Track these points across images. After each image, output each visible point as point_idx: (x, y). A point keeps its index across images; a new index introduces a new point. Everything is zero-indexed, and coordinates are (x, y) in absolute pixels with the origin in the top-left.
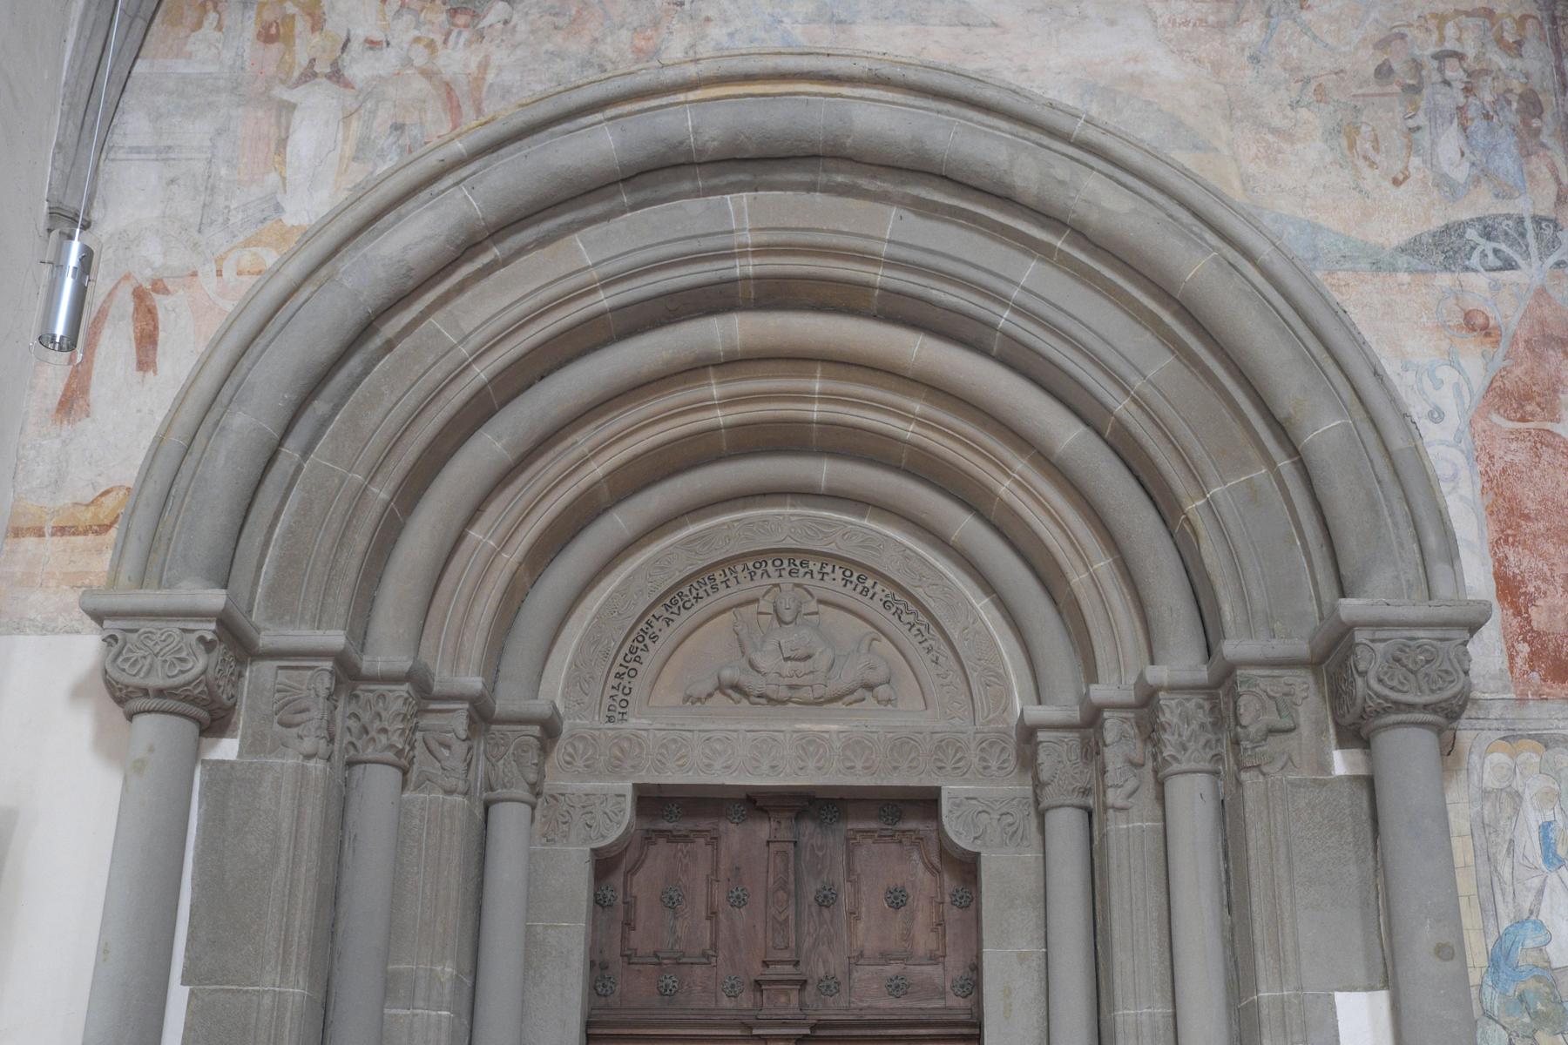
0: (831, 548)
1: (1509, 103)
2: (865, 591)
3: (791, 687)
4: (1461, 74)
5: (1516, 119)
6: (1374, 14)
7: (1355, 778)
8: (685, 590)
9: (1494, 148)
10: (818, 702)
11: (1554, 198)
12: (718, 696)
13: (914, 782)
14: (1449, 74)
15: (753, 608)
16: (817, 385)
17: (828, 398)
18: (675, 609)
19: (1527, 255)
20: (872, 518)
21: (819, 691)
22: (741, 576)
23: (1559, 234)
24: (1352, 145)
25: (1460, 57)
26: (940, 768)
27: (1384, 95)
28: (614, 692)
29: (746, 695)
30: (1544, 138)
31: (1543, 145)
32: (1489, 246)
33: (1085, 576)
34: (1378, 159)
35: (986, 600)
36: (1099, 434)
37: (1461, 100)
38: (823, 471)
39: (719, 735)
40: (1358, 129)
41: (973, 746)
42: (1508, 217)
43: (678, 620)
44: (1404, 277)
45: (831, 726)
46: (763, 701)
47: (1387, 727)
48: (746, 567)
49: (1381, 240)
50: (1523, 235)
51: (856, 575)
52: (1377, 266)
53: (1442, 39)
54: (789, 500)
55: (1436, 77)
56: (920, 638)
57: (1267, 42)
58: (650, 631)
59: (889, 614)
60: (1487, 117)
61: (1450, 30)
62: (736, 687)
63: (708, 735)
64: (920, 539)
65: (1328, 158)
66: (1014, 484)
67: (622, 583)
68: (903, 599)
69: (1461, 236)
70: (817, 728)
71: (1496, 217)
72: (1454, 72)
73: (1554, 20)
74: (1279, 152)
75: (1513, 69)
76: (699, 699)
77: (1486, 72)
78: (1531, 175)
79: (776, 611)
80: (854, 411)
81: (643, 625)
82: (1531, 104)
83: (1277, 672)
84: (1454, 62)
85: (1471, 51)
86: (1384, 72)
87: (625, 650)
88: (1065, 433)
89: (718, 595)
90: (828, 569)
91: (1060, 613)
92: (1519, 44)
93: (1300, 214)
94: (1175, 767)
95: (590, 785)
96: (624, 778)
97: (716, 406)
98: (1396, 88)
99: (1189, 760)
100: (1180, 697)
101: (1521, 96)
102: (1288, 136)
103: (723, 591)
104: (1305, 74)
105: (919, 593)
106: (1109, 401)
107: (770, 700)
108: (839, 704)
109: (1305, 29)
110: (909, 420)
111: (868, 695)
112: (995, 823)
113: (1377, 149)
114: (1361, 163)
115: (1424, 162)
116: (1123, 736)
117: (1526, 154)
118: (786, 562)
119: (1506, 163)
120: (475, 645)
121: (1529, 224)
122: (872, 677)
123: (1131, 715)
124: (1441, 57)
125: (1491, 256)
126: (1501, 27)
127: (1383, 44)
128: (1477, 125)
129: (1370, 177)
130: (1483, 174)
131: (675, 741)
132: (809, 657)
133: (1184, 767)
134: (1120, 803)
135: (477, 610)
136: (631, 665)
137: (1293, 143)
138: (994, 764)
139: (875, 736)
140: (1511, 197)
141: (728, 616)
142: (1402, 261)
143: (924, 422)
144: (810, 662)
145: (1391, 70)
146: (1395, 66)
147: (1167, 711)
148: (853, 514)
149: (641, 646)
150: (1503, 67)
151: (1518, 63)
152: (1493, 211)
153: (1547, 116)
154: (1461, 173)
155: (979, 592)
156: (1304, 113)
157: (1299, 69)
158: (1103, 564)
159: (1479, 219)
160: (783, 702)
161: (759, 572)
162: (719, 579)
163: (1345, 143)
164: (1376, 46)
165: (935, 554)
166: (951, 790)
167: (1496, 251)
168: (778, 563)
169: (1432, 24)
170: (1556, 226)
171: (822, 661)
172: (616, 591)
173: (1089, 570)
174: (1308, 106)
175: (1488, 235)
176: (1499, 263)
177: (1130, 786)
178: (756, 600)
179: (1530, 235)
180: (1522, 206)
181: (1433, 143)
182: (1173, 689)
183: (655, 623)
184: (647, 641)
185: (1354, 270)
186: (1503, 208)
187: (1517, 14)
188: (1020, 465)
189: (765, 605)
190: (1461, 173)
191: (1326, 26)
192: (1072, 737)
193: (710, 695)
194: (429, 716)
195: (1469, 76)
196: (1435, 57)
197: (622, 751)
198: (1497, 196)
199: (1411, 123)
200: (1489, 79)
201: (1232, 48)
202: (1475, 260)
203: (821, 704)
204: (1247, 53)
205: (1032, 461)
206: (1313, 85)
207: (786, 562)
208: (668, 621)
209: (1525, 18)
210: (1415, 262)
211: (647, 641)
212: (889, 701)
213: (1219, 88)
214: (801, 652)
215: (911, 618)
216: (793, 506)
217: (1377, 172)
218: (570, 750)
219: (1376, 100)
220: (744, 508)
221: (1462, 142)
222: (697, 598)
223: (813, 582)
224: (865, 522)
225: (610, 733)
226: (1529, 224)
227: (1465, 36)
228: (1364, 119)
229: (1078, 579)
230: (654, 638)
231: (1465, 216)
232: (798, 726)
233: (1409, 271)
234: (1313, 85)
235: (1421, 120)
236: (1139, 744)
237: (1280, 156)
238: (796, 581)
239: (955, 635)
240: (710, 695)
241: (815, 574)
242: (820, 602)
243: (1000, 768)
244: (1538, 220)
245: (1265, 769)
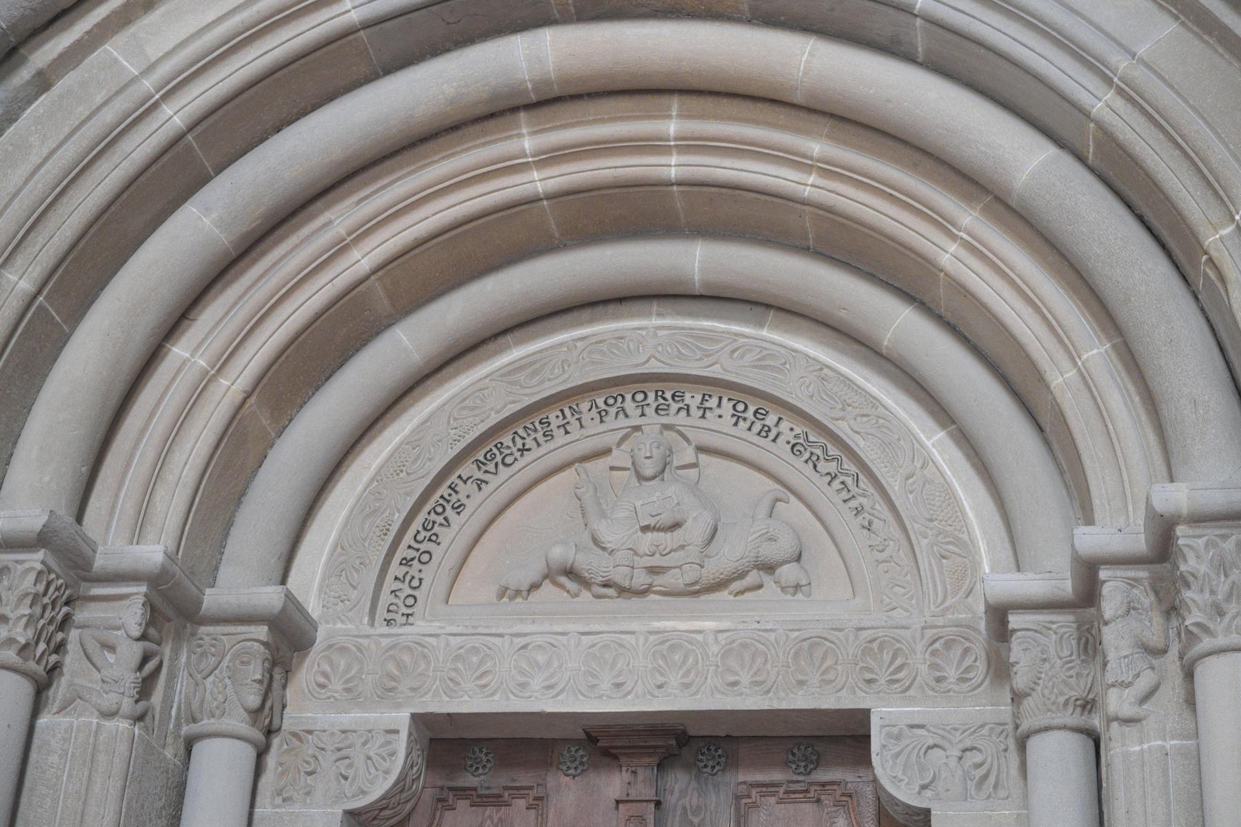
0: (716, 372)
2: (765, 431)
3: (654, 570)
8: (507, 440)
10: (697, 590)
12: (547, 587)
13: (828, 703)
15: (602, 464)
16: (672, 127)
17: (690, 145)
18: (491, 467)
20: (775, 327)
21: (691, 574)
22: (586, 417)
26: (869, 681)
28: (398, 585)
29: (585, 583)
33: (1071, 374)
35: (941, 435)
36: (1080, 158)
38: (695, 259)
39: (539, 640)
41: (920, 647)
43: (494, 481)
45: (706, 623)
46: (611, 592)
48: (594, 404)
51: (752, 409)
54: (655, 306)
56: (844, 495)
58: (454, 498)
59: (799, 462)
62: (570, 573)
63: (523, 641)
64: (843, 352)
66: (962, 247)
67: (413, 432)
68: (822, 441)
70: (683, 626)
76: (518, 592)
79: (633, 463)
80: (727, 162)
81: (444, 490)
87: (417, 524)
88: (1024, 158)
89: (552, 445)
90: (713, 402)
91: (1047, 443)
94: (1207, 643)
95: (351, 717)
96: (398, 706)
97: (529, 166)
99: (1228, 630)
100: (1211, 532)
103: (560, 438)
105: (842, 429)
106: (1084, 98)
107: (623, 591)
108: (724, 595)
110: (807, 168)
111: (767, 579)
112: (953, 762)
116: (1130, 608)
118: (651, 396)
120: (171, 505)
122: (770, 552)
123: (1142, 573)
131: (475, 650)
132: (676, 526)
133: (1221, 641)
134: (1127, 710)
135: (178, 458)
136: (423, 547)
138: (952, 673)
139: (772, 636)
141: (569, 474)
143: (828, 170)
144: (679, 533)
147: (1191, 556)
148: (746, 322)
149: (440, 519)
155: (930, 423)
158: (1097, 352)
160: (643, 593)
161: (613, 411)
162: (555, 422)
165: (867, 372)
166: (885, 715)
168: (640, 397)
171: (695, 531)
172: (406, 442)
173: (1075, 365)
177: (1143, 684)
178: (607, 452)
182: (1199, 519)
183: (461, 487)
184: (450, 512)
188: (969, 218)
189: (619, 457)
192: (1064, 621)
193: (534, 587)
194: (92, 605)
197: (400, 665)
203: (697, 593)
205: (986, 211)
207: (651, 396)
208: (480, 483)
211: (450, 512)
212: (797, 587)
214: (666, 519)
215: (832, 467)
216: (659, 315)
218: (327, 668)
220: (591, 321)
222: (523, 450)
223: (689, 421)
224: (765, 333)
225: (385, 642)
229: (1061, 379)
230: (459, 508)
232: (657, 625)
236: (1157, 619)
238: (665, 420)
239: (894, 486)
240: (534, 587)
241: (693, 410)
242: (701, 449)
243: (962, 680)
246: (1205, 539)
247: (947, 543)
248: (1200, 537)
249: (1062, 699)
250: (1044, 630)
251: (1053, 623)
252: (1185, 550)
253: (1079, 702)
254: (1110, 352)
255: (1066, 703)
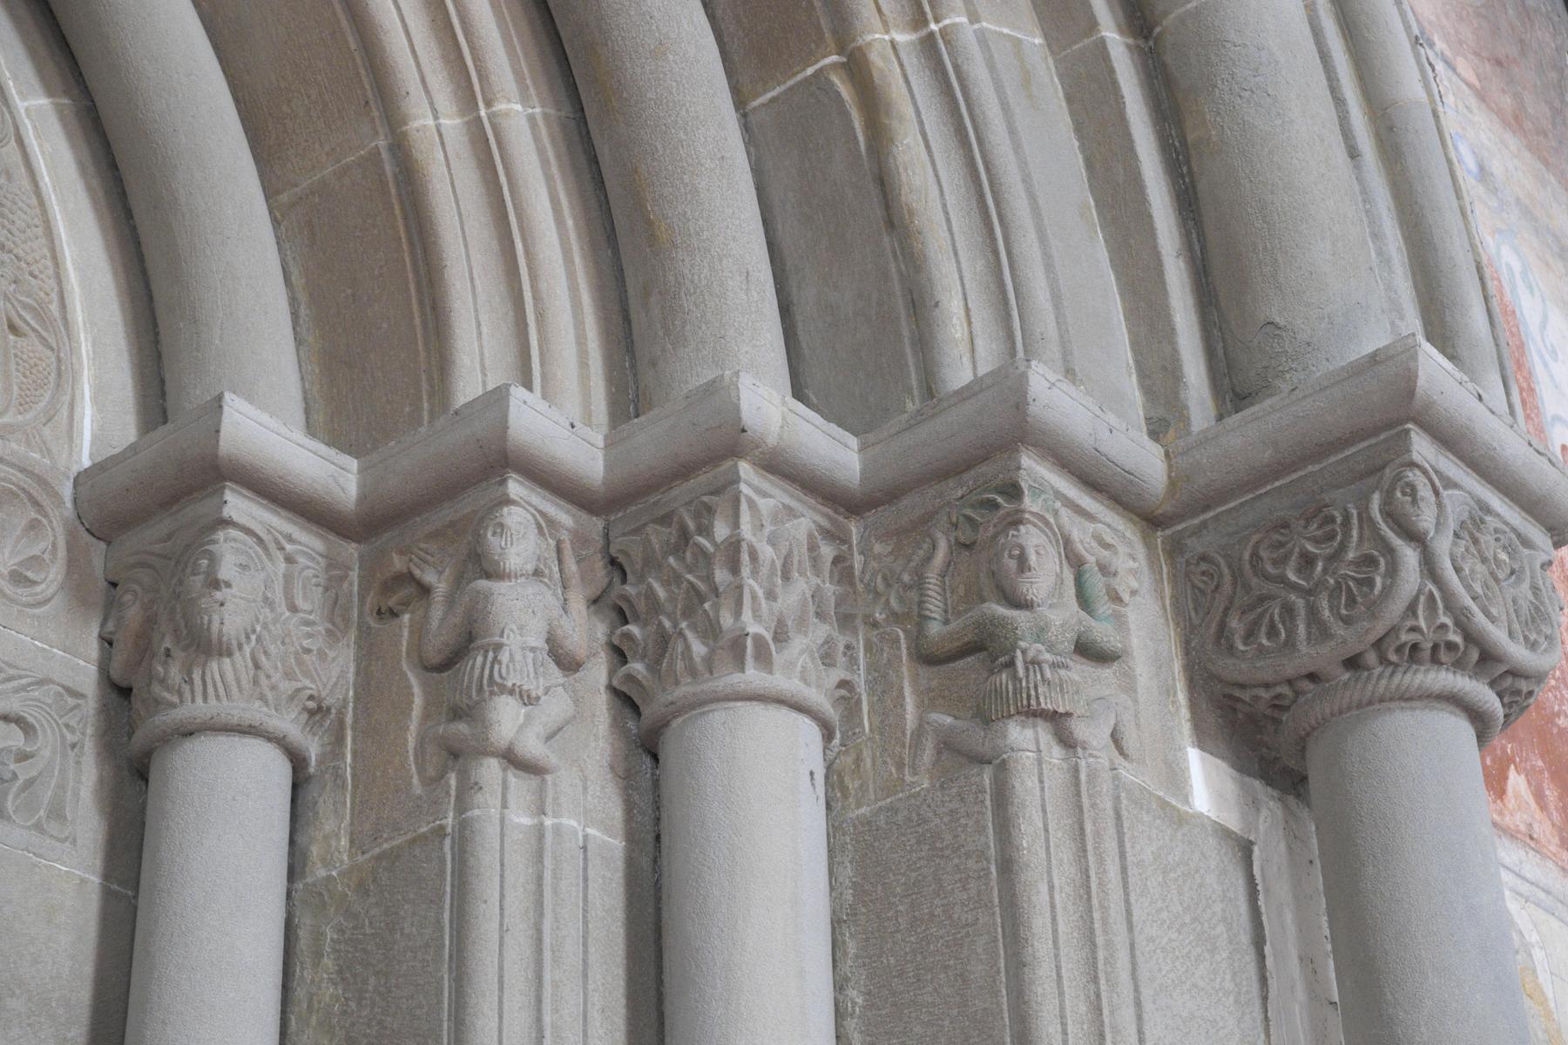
7: (1225, 833)
35: (42, 102)
47: (1408, 698)
83: (1087, 501)
91: (276, 222)
94: (752, 676)
123: (564, 516)
133: (780, 681)
134: (532, 746)
177: (557, 706)
245: (1080, 730)
246: (772, 502)
247: (25, 306)
248: (765, 495)
249: (287, 687)
250: (272, 547)
251: (290, 539)
252: (744, 506)
253: (312, 705)
254: (539, 119)
255: (292, 698)
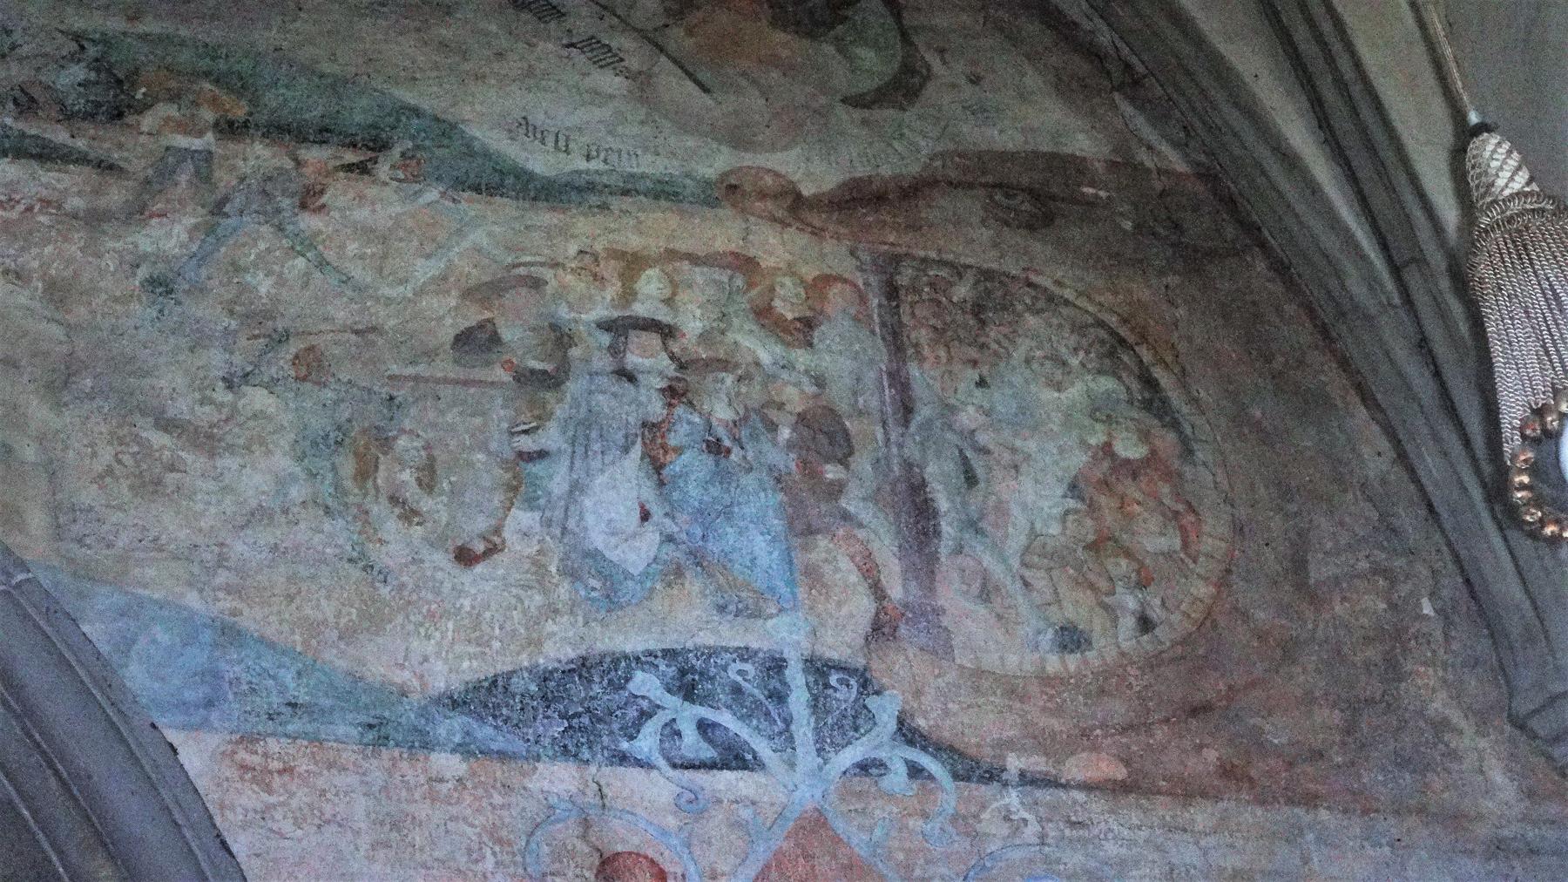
1: (773, 427)
4: (664, 362)
5: (788, 462)
6: (478, 237)
9: (727, 513)
11: (864, 623)
14: (633, 360)
19: (785, 737)
23: (873, 702)
24: (365, 473)
25: (667, 332)
27: (466, 383)
30: (851, 503)
31: (846, 517)
32: (688, 715)
34: (426, 504)
37: (656, 408)
40: (386, 443)
42: (745, 654)
44: (449, 764)
49: (402, 676)
50: (779, 697)
52: (378, 734)
53: (628, 295)
55: (603, 362)
57: (202, 259)
60: (715, 448)
61: (651, 284)
65: (296, 493)
69: (617, 686)
71: (713, 652)
72: (646, 356)
73: (892, 292)
74: (172, 468)
75: (788, 366)
77: (725, 365)
78: (813, 575)
82: (825, 434)
84: (654, 340)
85: (692, 323)
86: (476, 342)
92: (808, 324)
93: (193, 600)
98: (506, 377)
101: (802, 418)
102: (207, 441)
104: (280, 325)
109: (305, 244)
113: (428, 483)
114: (379, 508)
115: (548, 523)
117: (802, 529)
119: (755, 543)
121: (796, 677)
124: (620, 329)
125: (690, 736)
126: (772, 289)
127: (486, 292)
128: (692, 465)
129: (395, 542)
130: (689, 560)
137: (212, 455)
140: (757, 614)
142: (451, 726)
145: (495, 339)
146: (506, 334)
150: (765, 357)
151: (801, 357)
152: (707, 639)
153: (863, 463)
154: (638, 553)
156: (257, 398)
157: (268, 315)
159: (669, 654)
163: (348, 467)
164: (468, 294)
167: (704, 727)
169: (610, 269)
170: (865, 684)
174: (271, 386)
175: (688, 686)
176: (708, 753)
179: (799, 700)
180: (785, 634)
181: (576, 488)
185: (316, 740)
186: (731, 635)
187: (810, 272)
190: (638, 553)
191: (352, 248)
195: (682, 367)
196: (606, 326)
198: (722, 609)
199: (526, 443)
200: (730, 380)
201: (110, 263)
202: (647, 742)
204: (143, 272)
206: (294, 346)
209: (827, 280)
210: (484, 732)
213: (57, 331)
217: (418, 531)
219: (446, 392)
221: (648, 493)
226: (796, 677)
227: (683, 296)
228: (407, 424)
231: (634, 643)
233: (464, 749)
234: (294, 346)
235: (551, 437)
237: (171, 478)
244: (819, 668)
